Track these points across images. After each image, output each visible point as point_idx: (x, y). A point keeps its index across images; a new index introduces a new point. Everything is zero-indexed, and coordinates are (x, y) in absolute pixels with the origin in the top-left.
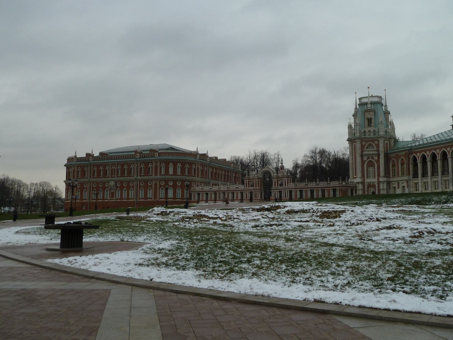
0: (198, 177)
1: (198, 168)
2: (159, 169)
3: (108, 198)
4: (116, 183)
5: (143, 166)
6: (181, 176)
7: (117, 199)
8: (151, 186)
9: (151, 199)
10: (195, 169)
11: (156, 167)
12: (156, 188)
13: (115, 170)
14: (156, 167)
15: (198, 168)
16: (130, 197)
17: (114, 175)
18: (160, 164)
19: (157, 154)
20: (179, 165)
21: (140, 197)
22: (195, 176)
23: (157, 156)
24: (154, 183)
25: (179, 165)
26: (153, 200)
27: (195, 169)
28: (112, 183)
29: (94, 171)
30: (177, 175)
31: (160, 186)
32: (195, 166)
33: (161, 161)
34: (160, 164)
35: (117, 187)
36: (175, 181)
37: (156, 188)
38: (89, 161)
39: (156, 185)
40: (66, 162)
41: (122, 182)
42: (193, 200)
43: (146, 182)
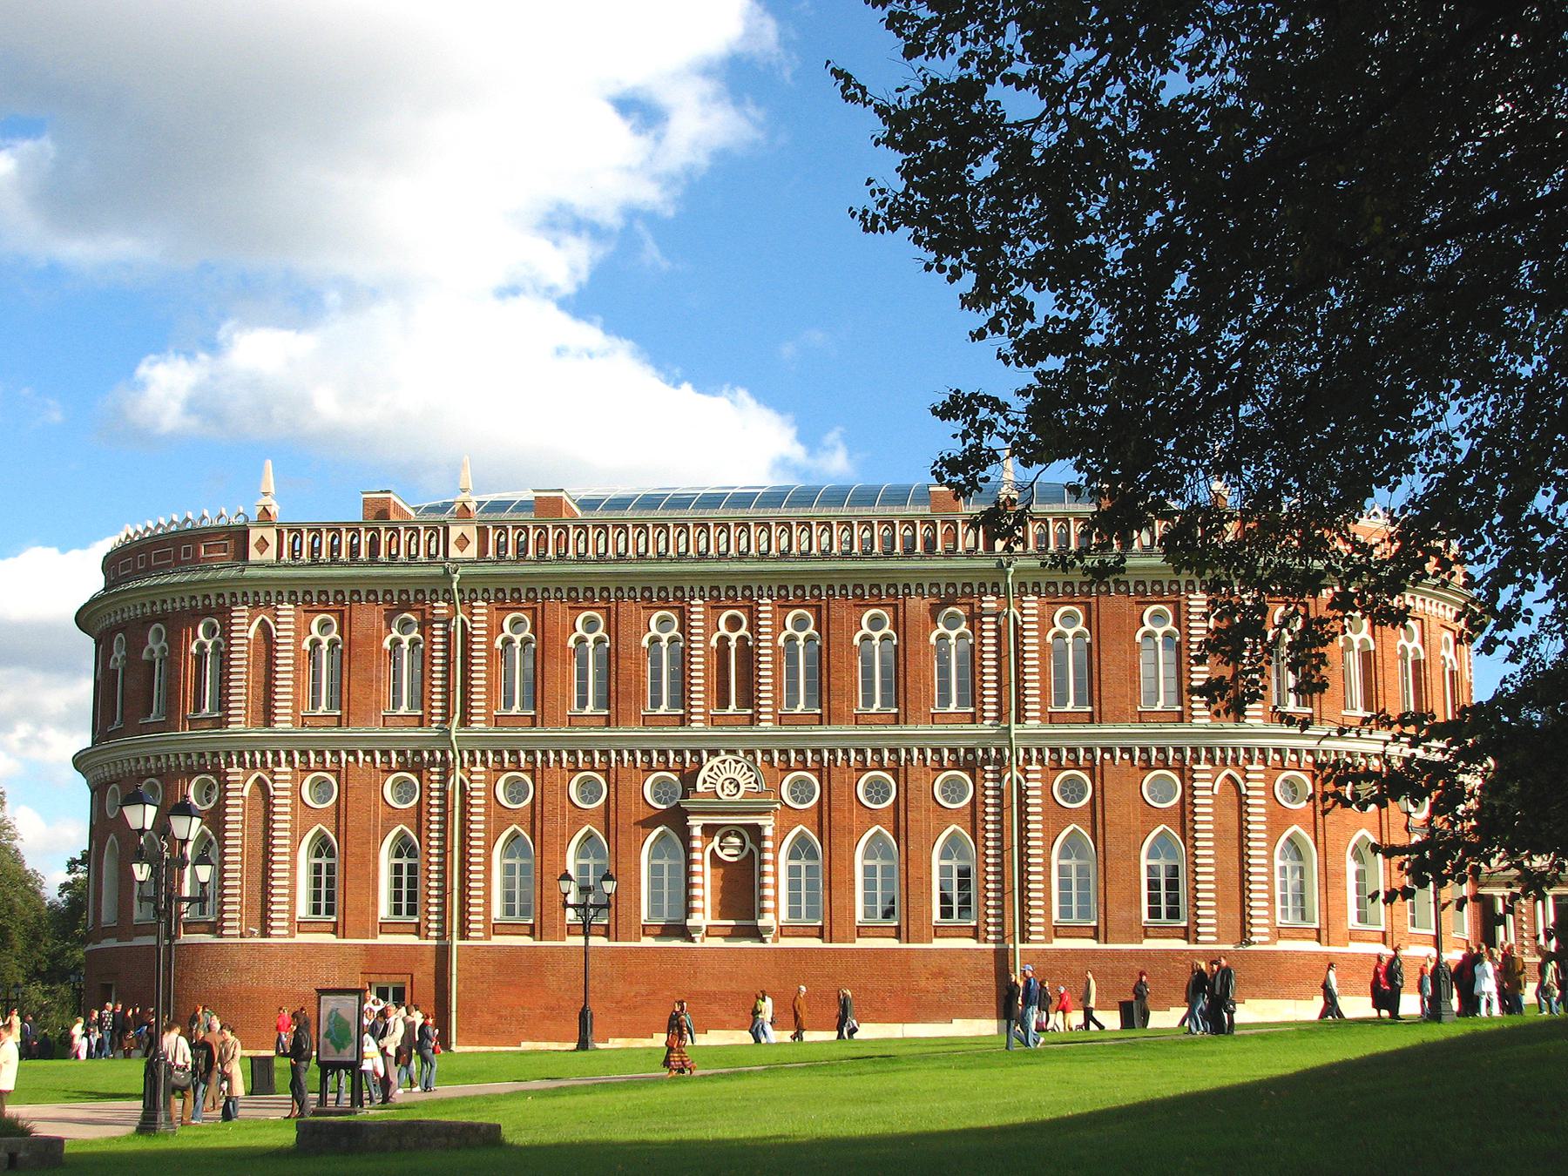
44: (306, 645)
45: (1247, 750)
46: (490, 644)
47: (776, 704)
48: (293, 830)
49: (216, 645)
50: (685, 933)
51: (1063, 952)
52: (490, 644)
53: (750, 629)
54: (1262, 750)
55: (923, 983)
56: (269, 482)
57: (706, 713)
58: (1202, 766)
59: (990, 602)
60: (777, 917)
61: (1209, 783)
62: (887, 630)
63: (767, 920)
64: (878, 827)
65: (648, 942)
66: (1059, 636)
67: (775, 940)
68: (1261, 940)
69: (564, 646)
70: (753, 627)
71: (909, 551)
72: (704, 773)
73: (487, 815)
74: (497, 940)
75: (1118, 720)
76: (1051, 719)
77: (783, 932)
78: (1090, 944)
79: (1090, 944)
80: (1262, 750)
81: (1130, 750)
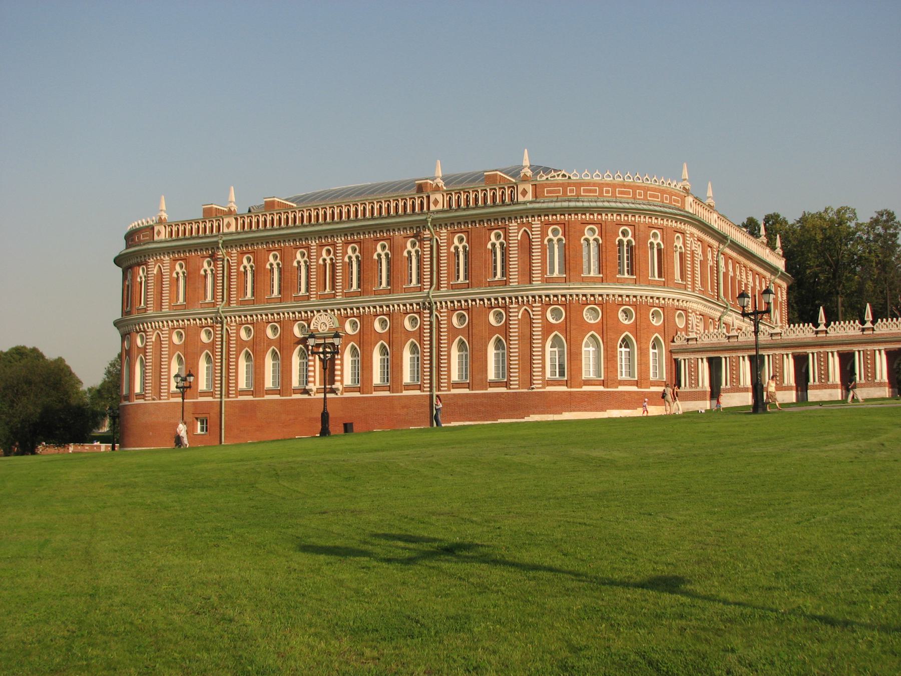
2: (536, 254)
8: (505, 330)
9: (507, 385)
13: (333, 265)
14: (527, 246)
15: (693, 252)
17: (333, 287)
19: (529, 188)
21: (455, 377)
22: (685, 288)
23: (529, 197)
24: (517, 314)
26: (515, 388)
31: (548, 328)
32: (684, 244)
34: (544, 234)
40: (120, 247)
42: (685, 387)
44: (452, 249)
45: (533, 297)
46: (238, 269)
47: (544, 272)
48: (169, 354)
49: (502, 244)
50: (306, 392)
51: (454, 395)
52: (238, 269)
53: (308, 257)
54: (540, 297)
55: (398, 411)
56: (232, 197)
57: (317, 294)
58: (514, 306)
59: (427, 234)
60: (342, 384)
61: (517, 314)
62: (560, 236)
63: (337, 385)
64: (460, 336)
65: (295, 396)
66: (550, 240)
67: (342, 394)
68: (538, 387)
69: (265, 268)
70: (335, 254)
71: (476, 206)
72: (313, 321)
73: (236, 344)
74: (241, 398)
75: (479, 286)
76: (453, 287)
77: (347, 389)
78: (467, 391)
79: (467, 391)
80: (540, 297)
81: (483, 300)
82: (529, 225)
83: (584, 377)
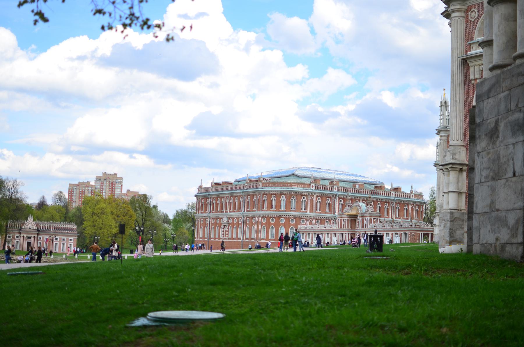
0: (311, 211)
1: (312, 201)
3: (222, 237)
4: (229, 218)
5: (249, 199)
6: (285, 211)
7: (229, 239)
10: (306, 203)
11: (259, 200)
12: (258, 226)
15: (312, 201)
16: (239, 237)
18: (263, 197)
20: (283, 199)
25: (283, 199)
27: (306, 203)
28: (225, 220)
29: (213, 204)
30: (280, 211)
31: (262, 224)
33: (265, 193)
34: (263, 197)
35: (229, 224)
36: (278, 218)
37: (258, 226)
38: (242, 188)
39: (258, 222)
41: (233, 218)
43: (252, 218)
82: (260, 194)
83: (270, 238)
